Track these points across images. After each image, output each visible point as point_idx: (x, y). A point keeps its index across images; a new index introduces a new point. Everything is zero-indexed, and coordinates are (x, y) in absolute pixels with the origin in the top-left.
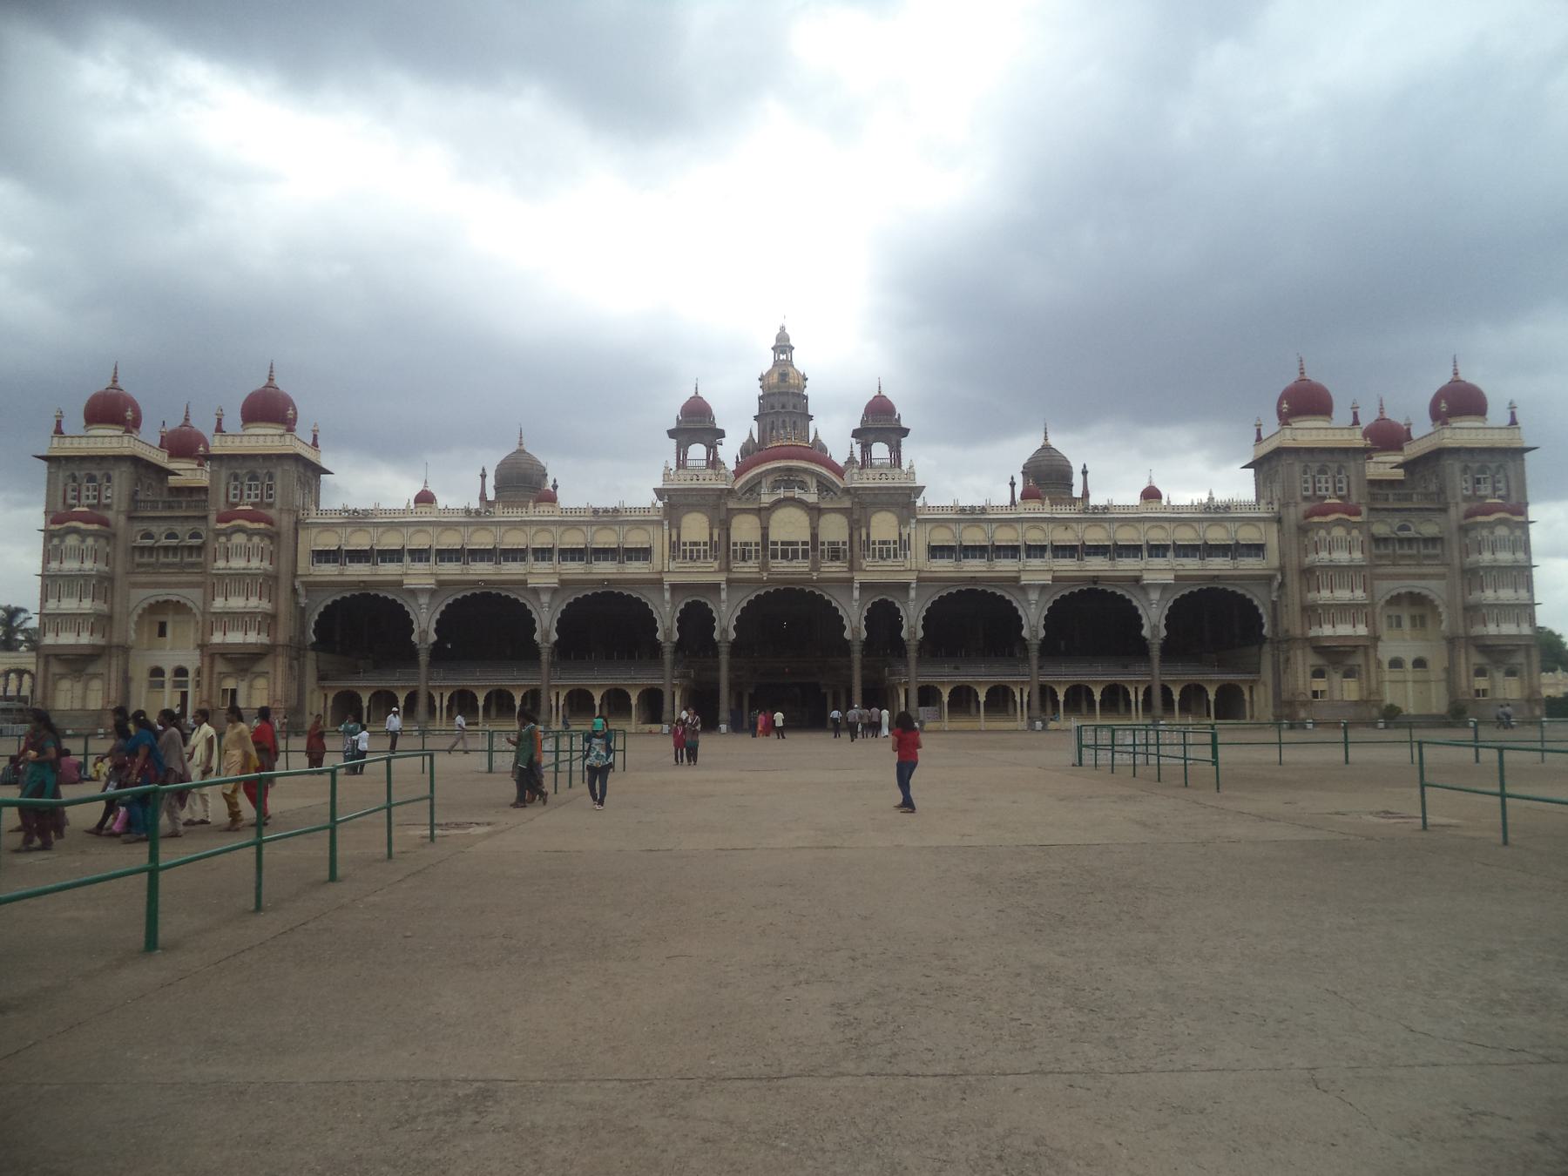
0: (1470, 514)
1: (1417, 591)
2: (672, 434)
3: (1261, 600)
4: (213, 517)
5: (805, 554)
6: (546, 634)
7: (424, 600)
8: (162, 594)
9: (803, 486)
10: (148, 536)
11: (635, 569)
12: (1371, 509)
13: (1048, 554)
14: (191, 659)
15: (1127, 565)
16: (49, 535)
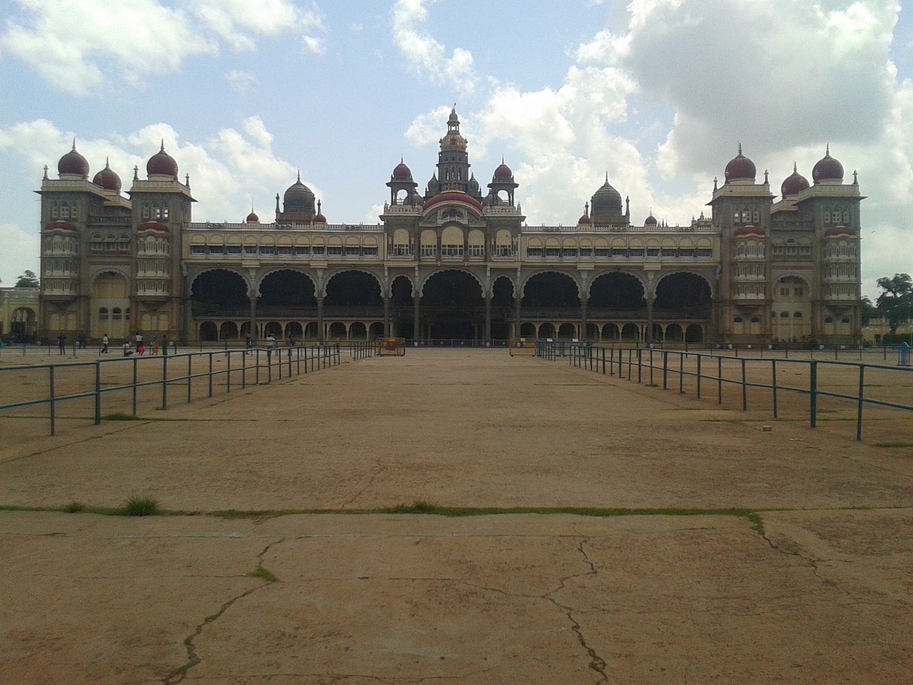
0: (827, 234)
1: (796, 275)
2: (388, 185)
4: (135, 227)
5: (461, 253)
6: (320, 293)
7: (253, 274)
9: (460, 215)
10: (98, 236)
11: (369, 259)
12: (771, 230)
13: (593, 253)
14: (124, 304)
15: (635, 260)
16: (44, 236)
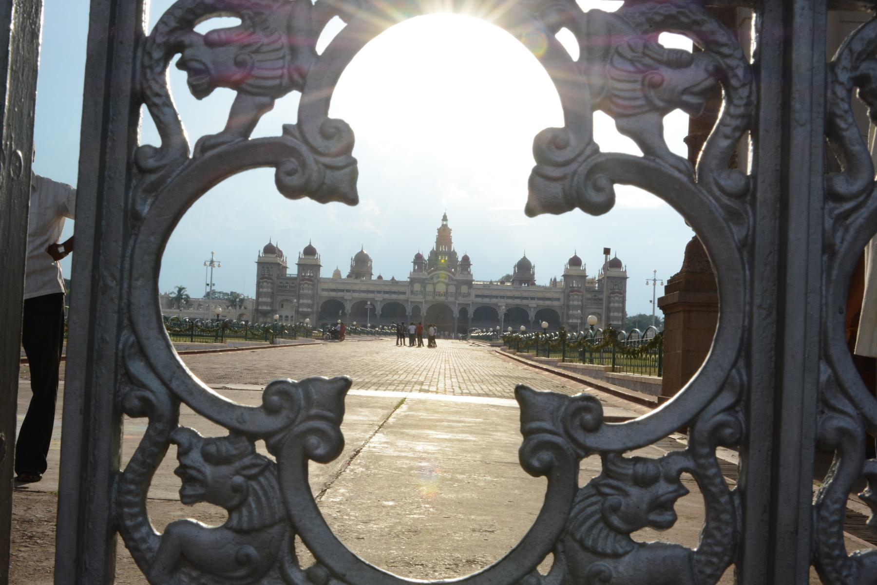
3: (559, 311)
8: (285, 297)
11: (402, 297)
15: (525, 302)
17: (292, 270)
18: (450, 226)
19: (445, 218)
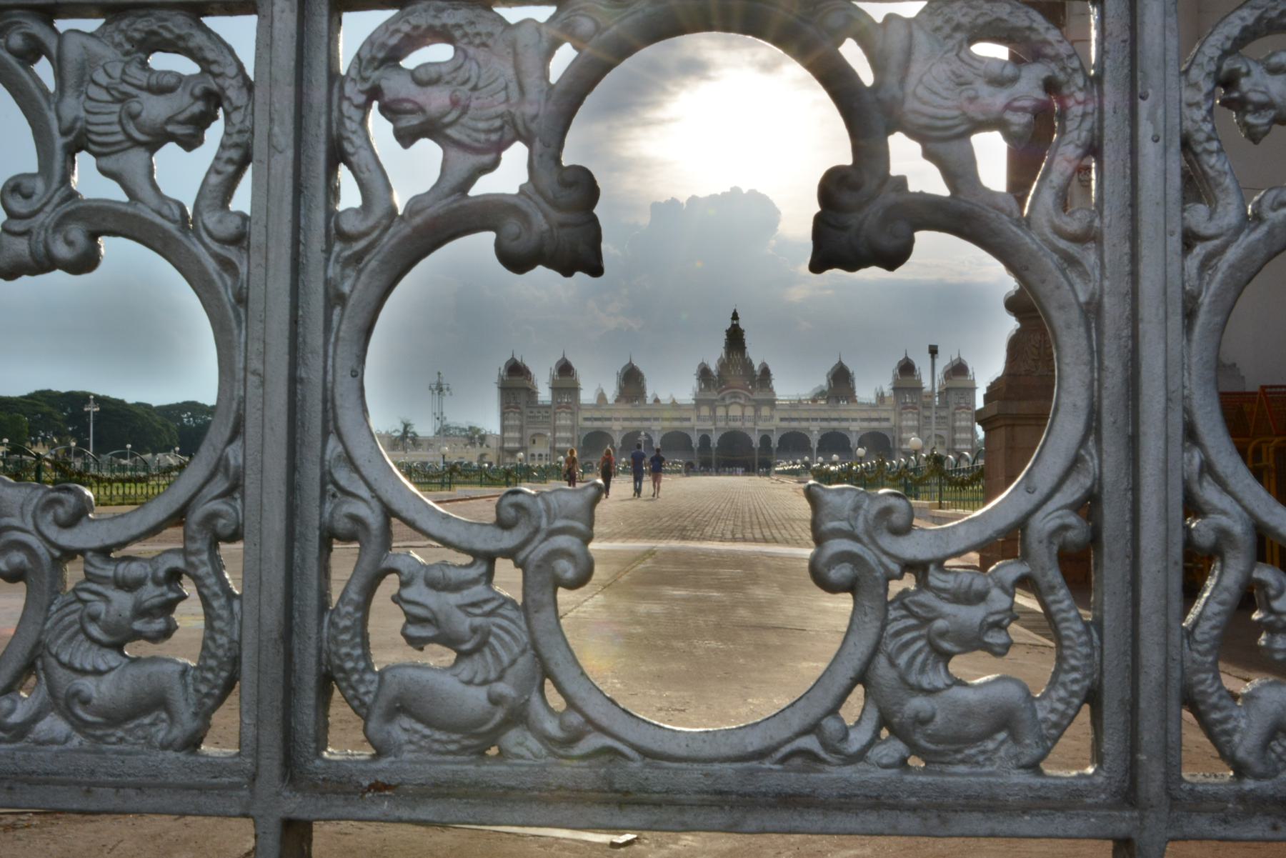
11: (686, 424)
15: (844, 424)
17: (544, 394)
18: (742, 326)
19: (735, 316)
